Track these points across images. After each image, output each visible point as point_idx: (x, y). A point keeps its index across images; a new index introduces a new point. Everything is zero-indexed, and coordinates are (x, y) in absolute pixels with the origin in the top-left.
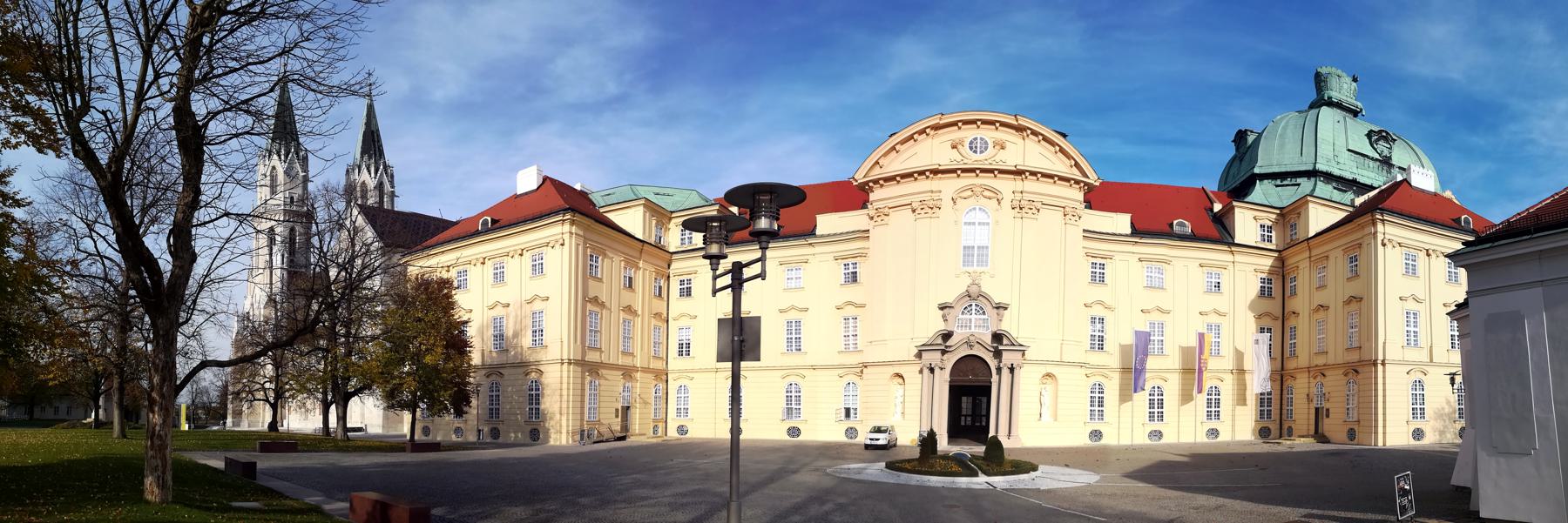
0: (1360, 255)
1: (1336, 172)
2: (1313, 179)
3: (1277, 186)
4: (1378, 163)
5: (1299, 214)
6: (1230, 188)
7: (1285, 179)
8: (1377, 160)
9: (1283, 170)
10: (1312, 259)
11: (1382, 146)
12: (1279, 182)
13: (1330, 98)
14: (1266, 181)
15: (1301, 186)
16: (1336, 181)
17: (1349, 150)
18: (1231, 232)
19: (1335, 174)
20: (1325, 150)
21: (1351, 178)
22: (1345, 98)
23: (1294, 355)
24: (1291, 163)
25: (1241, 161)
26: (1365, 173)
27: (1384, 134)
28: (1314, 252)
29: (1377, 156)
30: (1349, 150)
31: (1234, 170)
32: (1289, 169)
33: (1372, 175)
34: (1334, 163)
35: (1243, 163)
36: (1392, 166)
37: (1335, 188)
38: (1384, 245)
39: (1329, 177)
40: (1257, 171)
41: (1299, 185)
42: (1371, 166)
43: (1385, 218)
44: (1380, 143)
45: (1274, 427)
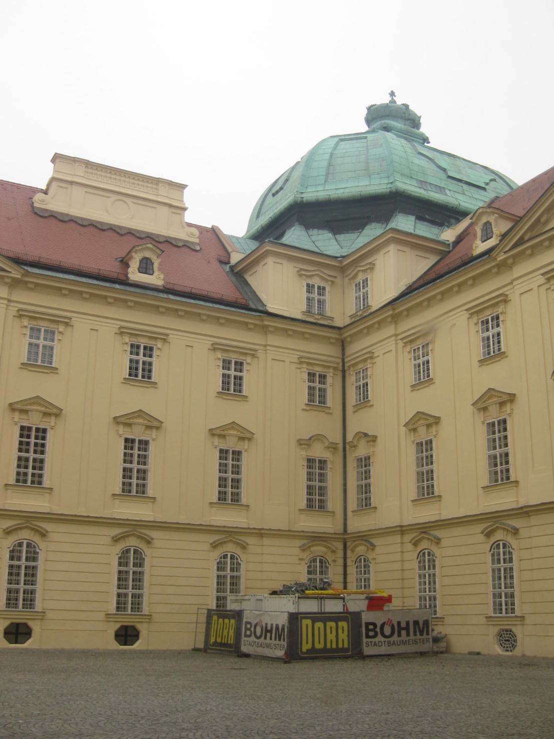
23: (366, 504)
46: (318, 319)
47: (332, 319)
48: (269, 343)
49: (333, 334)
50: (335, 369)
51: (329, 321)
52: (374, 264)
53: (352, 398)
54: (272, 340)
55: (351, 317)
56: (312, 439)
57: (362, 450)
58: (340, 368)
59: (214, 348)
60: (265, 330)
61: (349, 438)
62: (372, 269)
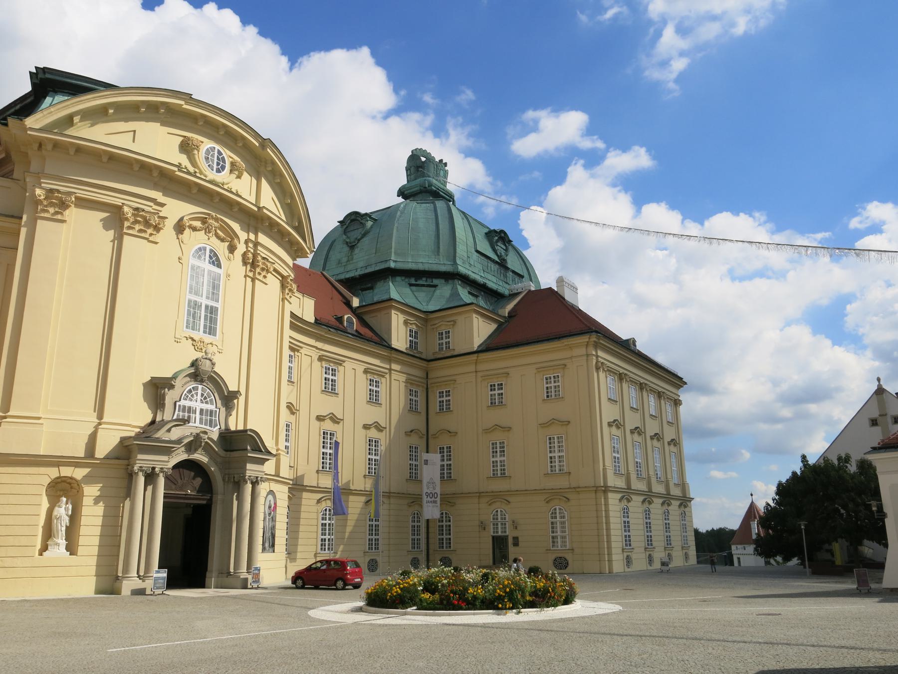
0: (563, 376)
1: (473, 276)
2: (450, 281)
3: (411, 285)
4: (497, 266)
5: (455, 322)
6: (342, 277)
7: (420, 278)
8: (496, 262)
9: (421, 267)
10: (480, 374)
11: (500, 247)
12: (413, 281)
13: (430, 185)
14: (398, 279)
15: (438, 288)
16: (470, 285)
17: (477, 251)
18: (385, 337)
19: (471, 277)
20: (461, 250)
21: (482, 282)
22: (442, 186)
24: (425, 261)
25: (352, 247)
26: (490, 277)
27: (503, 235)
28: (481, 367)
29: (496, 259)
30: (477, 251)
31: (335, 256)
32: (426, 267)
33: (494, 279)
34: (467, 266)
35: (356, 251)
36: (507, 269)
37: (469, 293)
38: (597, 369)
39: (466, 280)
40: (392, 265)
41: (435, 286)
42: (493, 269)
43: (601, 341)
44: (499, 244)
45: (422, 557)
46: (415, 353)
47: (421, 353)
48: (392, 368)
49: (424, 364)
50: (423, 387)
51: (420, 355)
52: (455, 322)
53: (434, 407)
54: (395, 366)
55: (434, 353)
56: (414, 431)
57: (445, 441)
58: (425, 386)
59: (366, 371)
60: (389, 360)
61: (431, 432)
62: (453, 325)
